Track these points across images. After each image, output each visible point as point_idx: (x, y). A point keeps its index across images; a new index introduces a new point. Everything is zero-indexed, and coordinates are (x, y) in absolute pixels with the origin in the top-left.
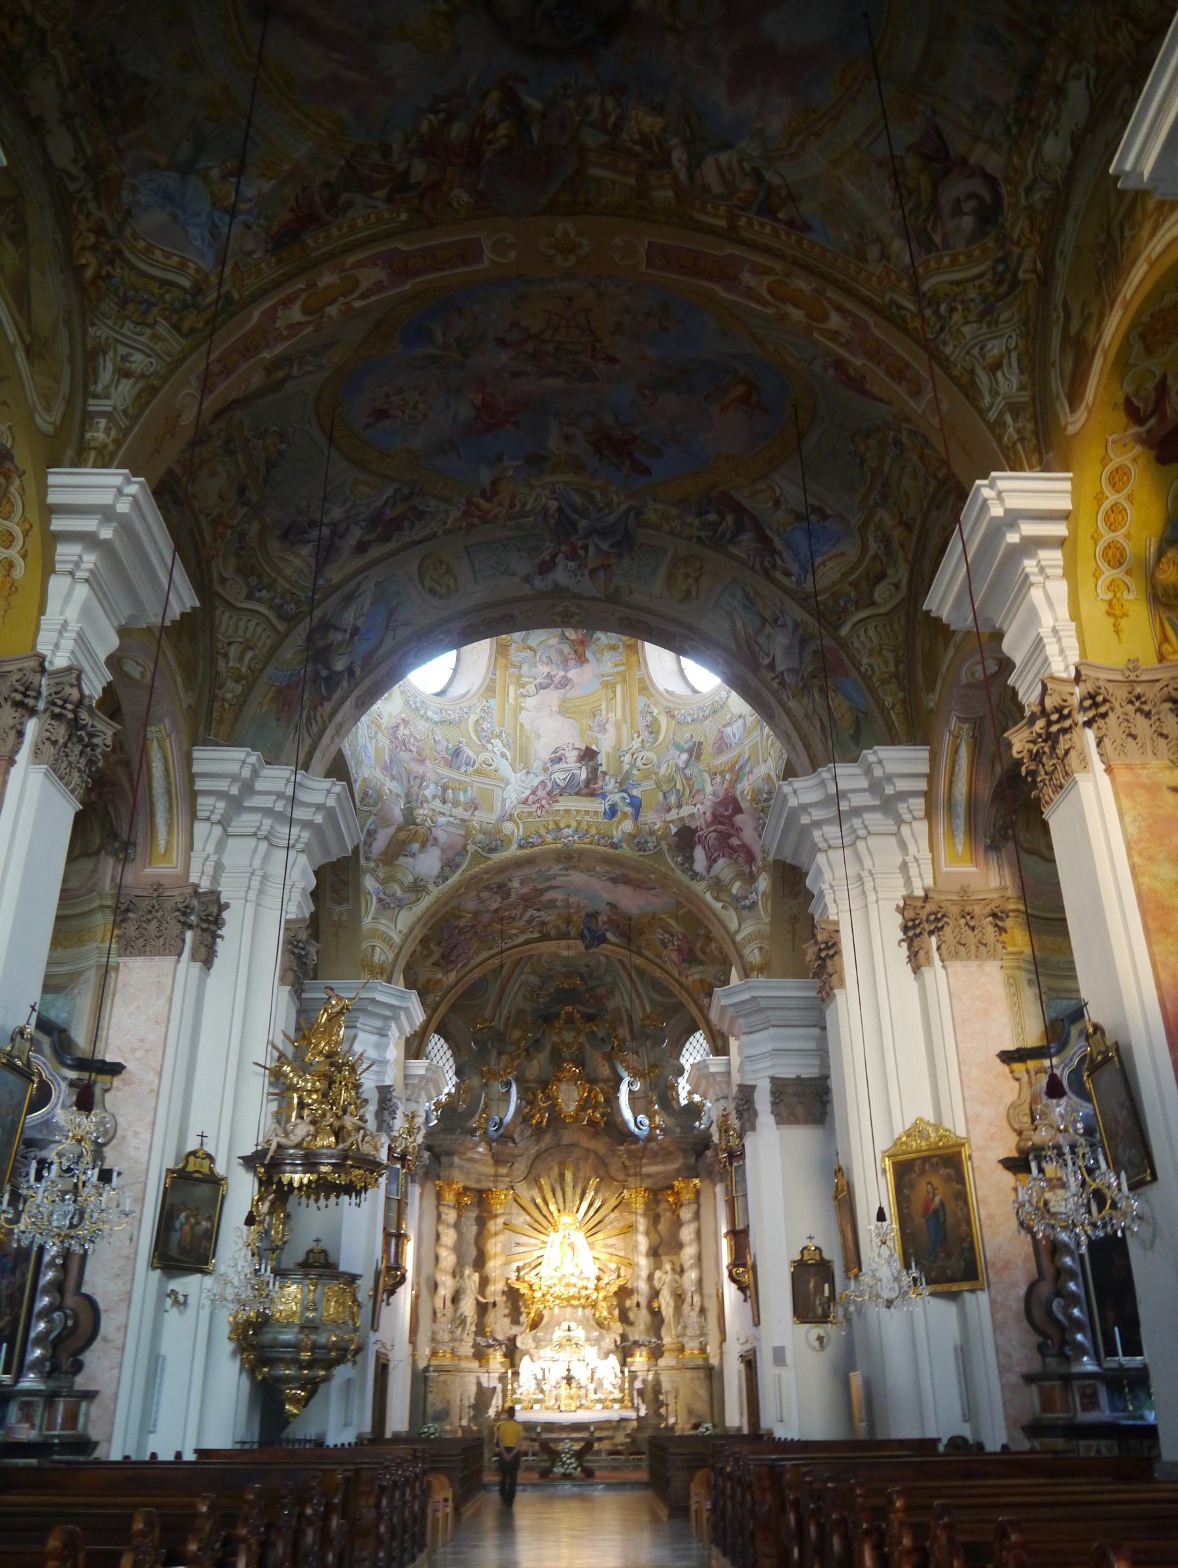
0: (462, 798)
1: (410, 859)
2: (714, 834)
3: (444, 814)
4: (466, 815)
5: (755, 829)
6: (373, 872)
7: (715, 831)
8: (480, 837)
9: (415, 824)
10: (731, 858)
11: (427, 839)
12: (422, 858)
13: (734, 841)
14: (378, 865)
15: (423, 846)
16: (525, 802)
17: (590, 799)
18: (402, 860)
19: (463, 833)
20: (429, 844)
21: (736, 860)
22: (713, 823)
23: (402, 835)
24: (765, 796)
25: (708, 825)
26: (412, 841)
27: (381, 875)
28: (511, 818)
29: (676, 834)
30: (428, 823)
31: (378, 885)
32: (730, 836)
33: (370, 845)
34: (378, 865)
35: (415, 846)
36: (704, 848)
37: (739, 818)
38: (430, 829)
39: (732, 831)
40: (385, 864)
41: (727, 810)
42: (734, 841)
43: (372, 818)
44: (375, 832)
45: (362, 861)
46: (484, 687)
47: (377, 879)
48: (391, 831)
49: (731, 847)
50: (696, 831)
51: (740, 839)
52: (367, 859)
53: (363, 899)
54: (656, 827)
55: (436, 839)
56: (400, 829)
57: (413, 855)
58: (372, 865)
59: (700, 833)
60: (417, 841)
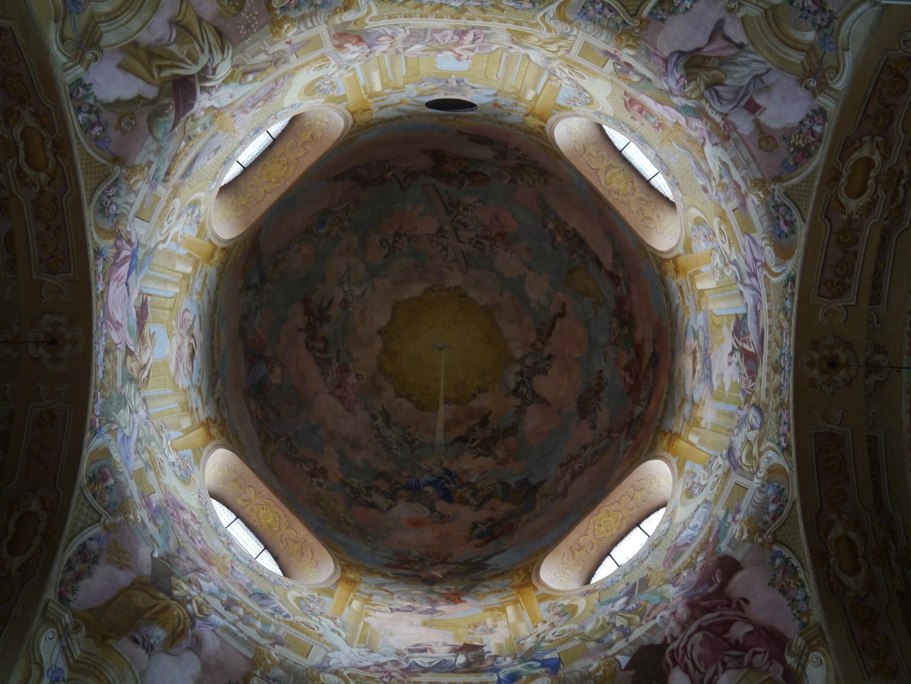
0: (259, 624)
1: (141, 652)
2: (699, 636)
3: (223, 617)
4: (263, 641)
5: (771, 584)
6: (64, 634)
7: (699, 629)
8: (279, 672)
9: (170, 594)
10: (739, 667)
11: (183, 633)
12: (164, 660)
13: (739, 631)
14: (77, 627)
15: (175, 638)
16: (366, 668)
17: (473, 675)
18: (125, 646)
19: (250, 655)
20: (185, 643)
21: (750, 666)
22: (692, 618)
23: (140, 599)
24: (772, 507)
25: (684, 626)
26: (153, 620)
27: (77, 652)
28: (336, 673)
29: (629, 666)
30: (193, 608)
31: (61, 664)
32: (727, 624)
33: (78, 577)
34: (77, 627)
35: (159, 634)
36: (686, 671)
37: (738, 584)
38: (192, 617)
39: (729, 613)
40: (90, 635)
41: (711, 584)
42: (739, 631)
43: (97, 529)
44: (95, 561)
45: (51, 594)
46: (320, 587)
47: (66, 651)
48: (125, 578)
49: (738, 646)
50: (665, 644)
51: (747, 621)
52: (63, 598)
53: (21, 663)
54: (591, 669)
55: (197, 645)
56: (138, 585)
57: (149, 649)
58: (67, 618)
59: (674, 645)
60: (163, 625)
